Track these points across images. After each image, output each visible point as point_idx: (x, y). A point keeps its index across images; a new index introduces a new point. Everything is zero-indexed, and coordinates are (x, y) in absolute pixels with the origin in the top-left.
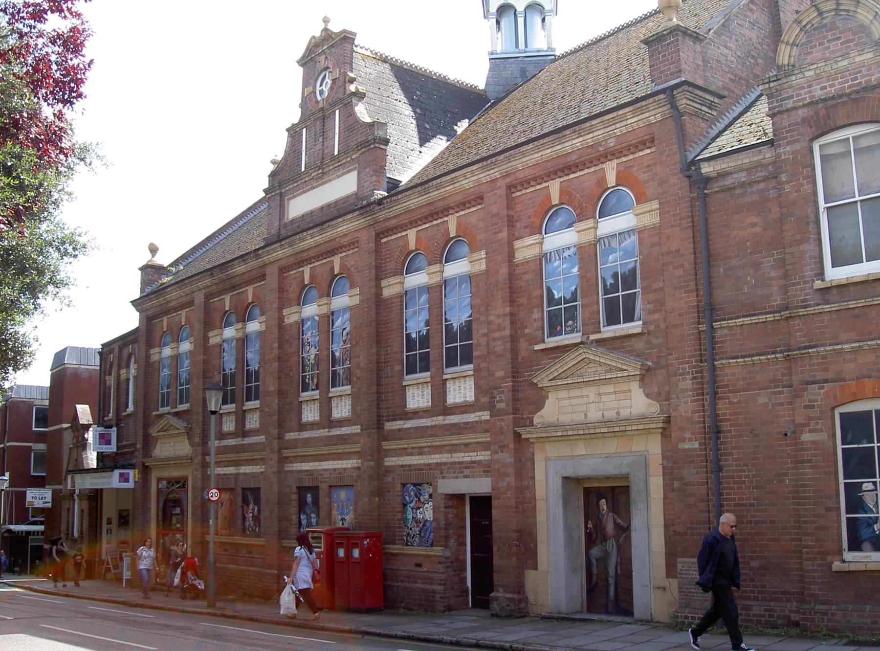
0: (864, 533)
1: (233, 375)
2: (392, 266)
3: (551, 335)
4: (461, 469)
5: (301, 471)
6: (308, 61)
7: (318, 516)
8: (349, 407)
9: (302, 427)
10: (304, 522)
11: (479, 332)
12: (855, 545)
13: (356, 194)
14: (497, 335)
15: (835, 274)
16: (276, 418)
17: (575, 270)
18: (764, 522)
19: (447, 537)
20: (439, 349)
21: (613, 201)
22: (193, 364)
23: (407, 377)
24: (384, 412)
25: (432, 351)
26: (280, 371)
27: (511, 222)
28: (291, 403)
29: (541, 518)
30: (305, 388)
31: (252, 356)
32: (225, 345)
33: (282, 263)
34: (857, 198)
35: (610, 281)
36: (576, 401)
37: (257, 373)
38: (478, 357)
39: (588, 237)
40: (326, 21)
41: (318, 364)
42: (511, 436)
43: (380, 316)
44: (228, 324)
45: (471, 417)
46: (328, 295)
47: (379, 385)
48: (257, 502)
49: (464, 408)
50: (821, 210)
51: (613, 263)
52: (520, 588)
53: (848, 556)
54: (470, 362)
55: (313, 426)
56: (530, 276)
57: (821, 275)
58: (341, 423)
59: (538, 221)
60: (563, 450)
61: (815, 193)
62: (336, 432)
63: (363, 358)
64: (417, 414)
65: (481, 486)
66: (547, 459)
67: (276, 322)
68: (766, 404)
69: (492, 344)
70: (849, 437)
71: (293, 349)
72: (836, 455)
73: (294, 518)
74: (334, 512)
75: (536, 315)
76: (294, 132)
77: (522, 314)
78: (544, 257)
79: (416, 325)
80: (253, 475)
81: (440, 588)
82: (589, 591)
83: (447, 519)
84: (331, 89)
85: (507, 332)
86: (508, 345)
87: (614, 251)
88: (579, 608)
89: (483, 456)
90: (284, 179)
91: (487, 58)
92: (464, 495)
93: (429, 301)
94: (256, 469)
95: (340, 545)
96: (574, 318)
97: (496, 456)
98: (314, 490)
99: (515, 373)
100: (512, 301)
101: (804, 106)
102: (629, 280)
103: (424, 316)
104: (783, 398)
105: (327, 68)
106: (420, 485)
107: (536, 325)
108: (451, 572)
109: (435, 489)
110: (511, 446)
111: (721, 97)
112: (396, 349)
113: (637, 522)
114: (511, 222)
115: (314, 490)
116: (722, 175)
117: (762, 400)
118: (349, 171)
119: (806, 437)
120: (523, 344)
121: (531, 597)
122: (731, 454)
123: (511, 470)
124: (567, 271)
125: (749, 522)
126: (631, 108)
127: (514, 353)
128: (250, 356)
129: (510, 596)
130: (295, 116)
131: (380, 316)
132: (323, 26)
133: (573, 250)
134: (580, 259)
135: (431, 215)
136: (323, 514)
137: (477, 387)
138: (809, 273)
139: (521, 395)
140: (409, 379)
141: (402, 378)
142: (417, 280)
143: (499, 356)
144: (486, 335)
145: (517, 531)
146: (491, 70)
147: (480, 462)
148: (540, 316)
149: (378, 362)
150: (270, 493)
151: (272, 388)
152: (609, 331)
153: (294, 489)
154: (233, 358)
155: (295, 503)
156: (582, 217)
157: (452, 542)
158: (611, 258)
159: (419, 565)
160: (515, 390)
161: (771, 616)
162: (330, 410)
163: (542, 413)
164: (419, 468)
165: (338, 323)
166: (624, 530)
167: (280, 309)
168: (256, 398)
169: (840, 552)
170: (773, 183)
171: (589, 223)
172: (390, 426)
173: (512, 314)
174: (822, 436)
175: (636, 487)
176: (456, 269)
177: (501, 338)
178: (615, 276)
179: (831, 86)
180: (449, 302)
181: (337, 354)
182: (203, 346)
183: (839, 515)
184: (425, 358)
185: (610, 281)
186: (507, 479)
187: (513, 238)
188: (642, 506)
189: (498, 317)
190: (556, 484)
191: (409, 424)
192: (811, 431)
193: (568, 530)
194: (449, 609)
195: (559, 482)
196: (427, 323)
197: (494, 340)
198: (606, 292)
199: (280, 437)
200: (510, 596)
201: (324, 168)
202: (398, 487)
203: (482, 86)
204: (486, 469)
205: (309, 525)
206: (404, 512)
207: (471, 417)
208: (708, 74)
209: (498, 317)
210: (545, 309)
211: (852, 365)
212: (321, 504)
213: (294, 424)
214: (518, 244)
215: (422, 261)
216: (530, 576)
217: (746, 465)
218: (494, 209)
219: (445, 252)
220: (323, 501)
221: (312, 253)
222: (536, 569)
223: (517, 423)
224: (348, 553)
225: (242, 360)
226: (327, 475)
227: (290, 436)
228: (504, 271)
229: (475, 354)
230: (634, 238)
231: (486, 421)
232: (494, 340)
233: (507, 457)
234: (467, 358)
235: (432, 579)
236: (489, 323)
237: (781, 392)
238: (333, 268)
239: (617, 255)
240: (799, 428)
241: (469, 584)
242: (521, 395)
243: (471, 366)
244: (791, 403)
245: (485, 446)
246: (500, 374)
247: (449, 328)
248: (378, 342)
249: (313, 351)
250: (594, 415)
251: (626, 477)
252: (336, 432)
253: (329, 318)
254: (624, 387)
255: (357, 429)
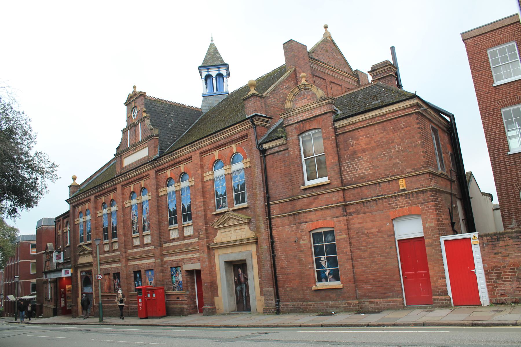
0: (322, 275)
1: (107, 228)
2: (162, 184)
3: (218, 208)
4: (191, 260)
5: (134, 265)
6: (127, 104)
7: (141, 282)
8: (150, 239)
9: (134, 247)
10: (137, 285)
11: (193, 208)
12: (320, 280)
13: (148, 156)
14: (199, 209)
15: (309, 184)
16: (123, 245)
17: (225, 184)
18: (290, 274)
19: (187, 287)
20: (180, 215)
21: (236, 158)
22: (92, 224)
23: (170, 226)
24: (162, 240)
25: (178, 216)
26: (124, 226)
27: (202, 167)
28: (129, 238)
29: (218, 277)
30: (134, 232)
31: (114, 220)
32: (104, 217)
33: (123, 183)
34: (315, 156)
35: (236, 188)
36: (227, 233)
37: (116, 227)
38: (194, 218)
39: (228, 172)
40: (135, 87)
41: (138, 222)
42: (206, 247)
43: (159, 201)
44: (104, 208)
45: (192, 241)
46: (140, 196)
47: (160, 229)
48: (119, 278)
49: (190, 237)
50: (303, 160)
51: (238, 181)
52: (212, 304)
53: (318, 284)
54: (191, 220)
55: (138, 246)
56: (210, 187)
57: (303, 184)
58: (148, 245)
59: (211, 166)
60: (224, 251)
61: (300, 154)
62: (146, 249)
63: (155, 219)
64: (174, 240)
65: (196, 266)
66: (219, 255)
67: (121, 207)
68: (288, 231)
69: (198, 213)
70: (316, 241)
71: (128, 217)
72: (311, 248)
73: (133, 283)
74: (147, 280)
75: (212, 201)
76: (124, 131)
77: (208, 201)
78: (213, 180)
79: (172, 207)
80: (117, 268)
81: (186, 306)
82: (237, 303)
83: (187, 280)
84: (137, 115)
85: (202, 208)
86: (203, 213)
87: (237, 177)
88: (234, 310)
89: (197, 255)
90: (121, 152)
91: (202, 96)
92: (193, 270)
93: (176, 197)
94: (118, 265)
95: (148, 293)
96: (225, 202)
97: (201, 255)
98: (139, 272)
99: (206, 223)
100: (204, 196)
101: (295, 123)
102: (242, 187)
103: (174, 203)
104: (293, 229)
105: (135, 107)
106: (177, 267)
107: (212, 205)
108: (190, 300)
109: (182, 269)
110: (206, 251)
111: (271, 118)
112: (165, 216)
113: (250, 276)
114: (202, 167)
115: (139, 272)
116: (271, 148)
117: (287, 230)
118: (145, 147)
119: (302, 242)
120: (208, 212)
121: (217, 307)
122: (278, 250)
123: (207, 260)
124: (222, 184)
125: (285, 274)
126: (239, 124)
127: (205, 216)
128: (113, 220)
129: (209, 307)
130: (125, 125)
131: (159, 201)
132: (133, 90)
133: (224, 176)
134: (226, 180)
135: (175, 164)
136: (143, 281)
137: (194, 229)
138: (300, 185)
139: (209, 231)
140: (171, 227)
141: (168, 227)
142: (171, 189)
143: (201, 217)
144: (196, 209)
145: (210, 283)
146: (203, 101)
147: (196, 257)
148: (213, 202)
149: (159, 221)
150: (123, 275)
151: (121, 233)
152: (237, 206)
153: (132, 272)
154: (107, 222)
155: (133, 278)
156: (225, 164)
157: (190, 288)
158: (236, 179)
159: (178, 298)
160: (206, 230)
161: (295, 307)
162: (144, 240)
163: (216, 238)
164: (176, 261)
165: (144, 206)
166: (246, 279)
167: (123, 202)
168: (116, 237)
169: (315, 283)
170: (286, 151)
171: (228, 167)
172: (165, 245)
173: (204, 201)
174: (306, 242)
175: (248, 263)
176: (184, 184)
177: (200, 210)
178: (238, 186)
179: (304, 116)
180: (182, 197)
181: (145, 218)
182: (95, 217)
183: (314, 270)
184: (176, 218)
185: (236, 188)
186: (206, 263)
187: (203, 172)
188: (251, 270)
189: (199, 202)
190: (223, 264)
191: (171, 244)
192: (303, 240)
193: (228, 281)
194: (191, 314)
195: (223, 263)
196: (176, 206)
197: (198, 211)
198: (235, 192)
199: (126, 252)
200: (209, 307)
201: (136, 147)
202: (169, 269)
203: (200, 108)
204: (199, 260)
205: (139, 286)
206: (172, 278)
207: (192, 241)
208: (267, 110)
209: (199, 202)
210: (216, 199)
211: (315, 216)
212: (142, 277)
213: (131, 246)
214: (205, 175)
215: (172, 181)
216: (216, 298)
217: (283, 253)
218: (196, 162)
219: (182, 177)
220: (143, 276)
221: (133, 179)
222: (218, 296)
223: (207, 242)
224: (151, 296)
225: (110, 222)
226: (143, 266)
227: (129, 251)
228: (200, 185)
229: (193, 216)
230: (243, 172)
231: (198, 242)
232: (198, 211)
233: (205, 255)
234: (190, 219)
235: (183, 303)
236: (196, 205)
237: (293, 227)
238: (141, 185)
239: (238, 178)
240: (299, 239)
241: (197, 304)
242: (209, 231)
243: (191, 221)
244: (296, 230)
245: (197, 251)
246: (201, 224)
247: (183, 207)
248: (158, 214)
249: (136, 218)
250: (234, 238)
251: (245, 260)
252: (146, 249)
253: (141, 204)
254: (242, 227)
255: (153, 247)
